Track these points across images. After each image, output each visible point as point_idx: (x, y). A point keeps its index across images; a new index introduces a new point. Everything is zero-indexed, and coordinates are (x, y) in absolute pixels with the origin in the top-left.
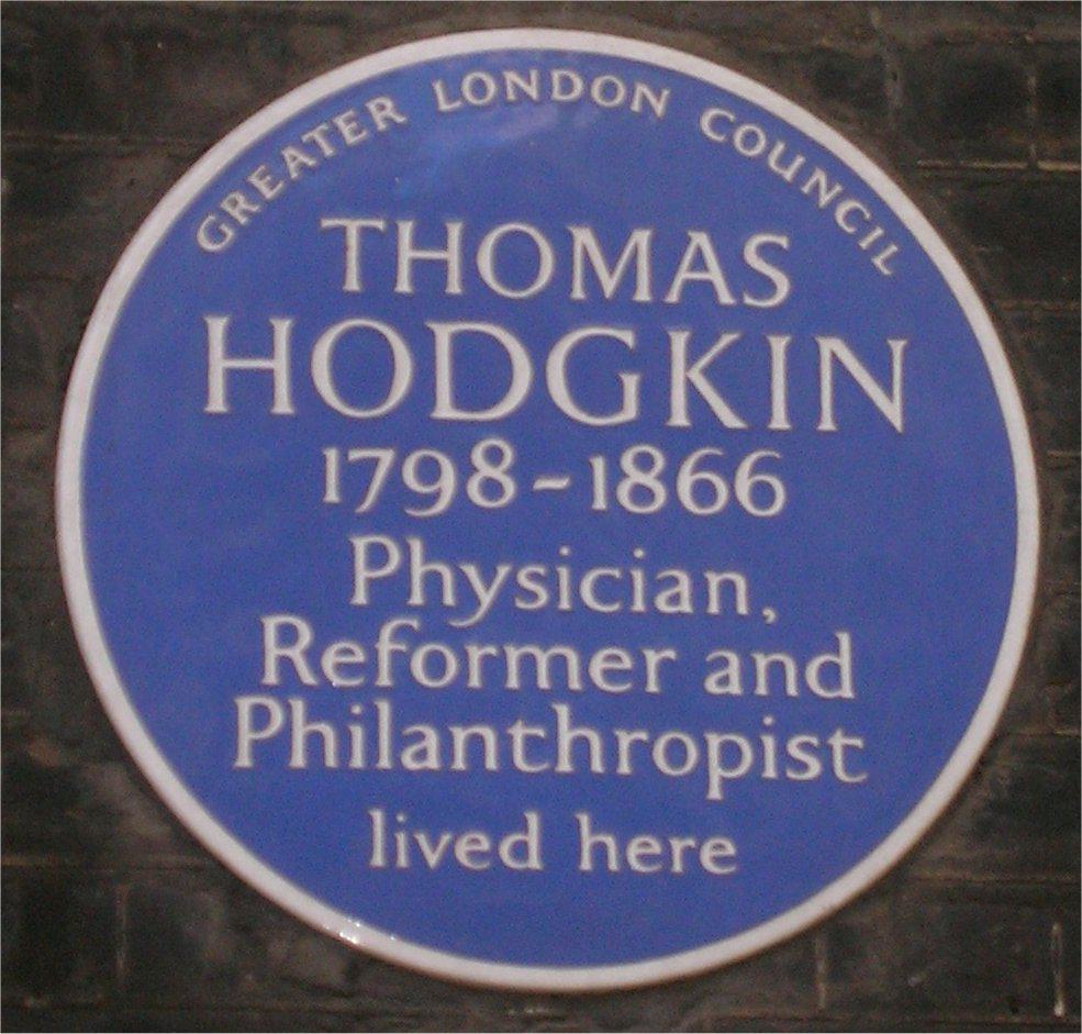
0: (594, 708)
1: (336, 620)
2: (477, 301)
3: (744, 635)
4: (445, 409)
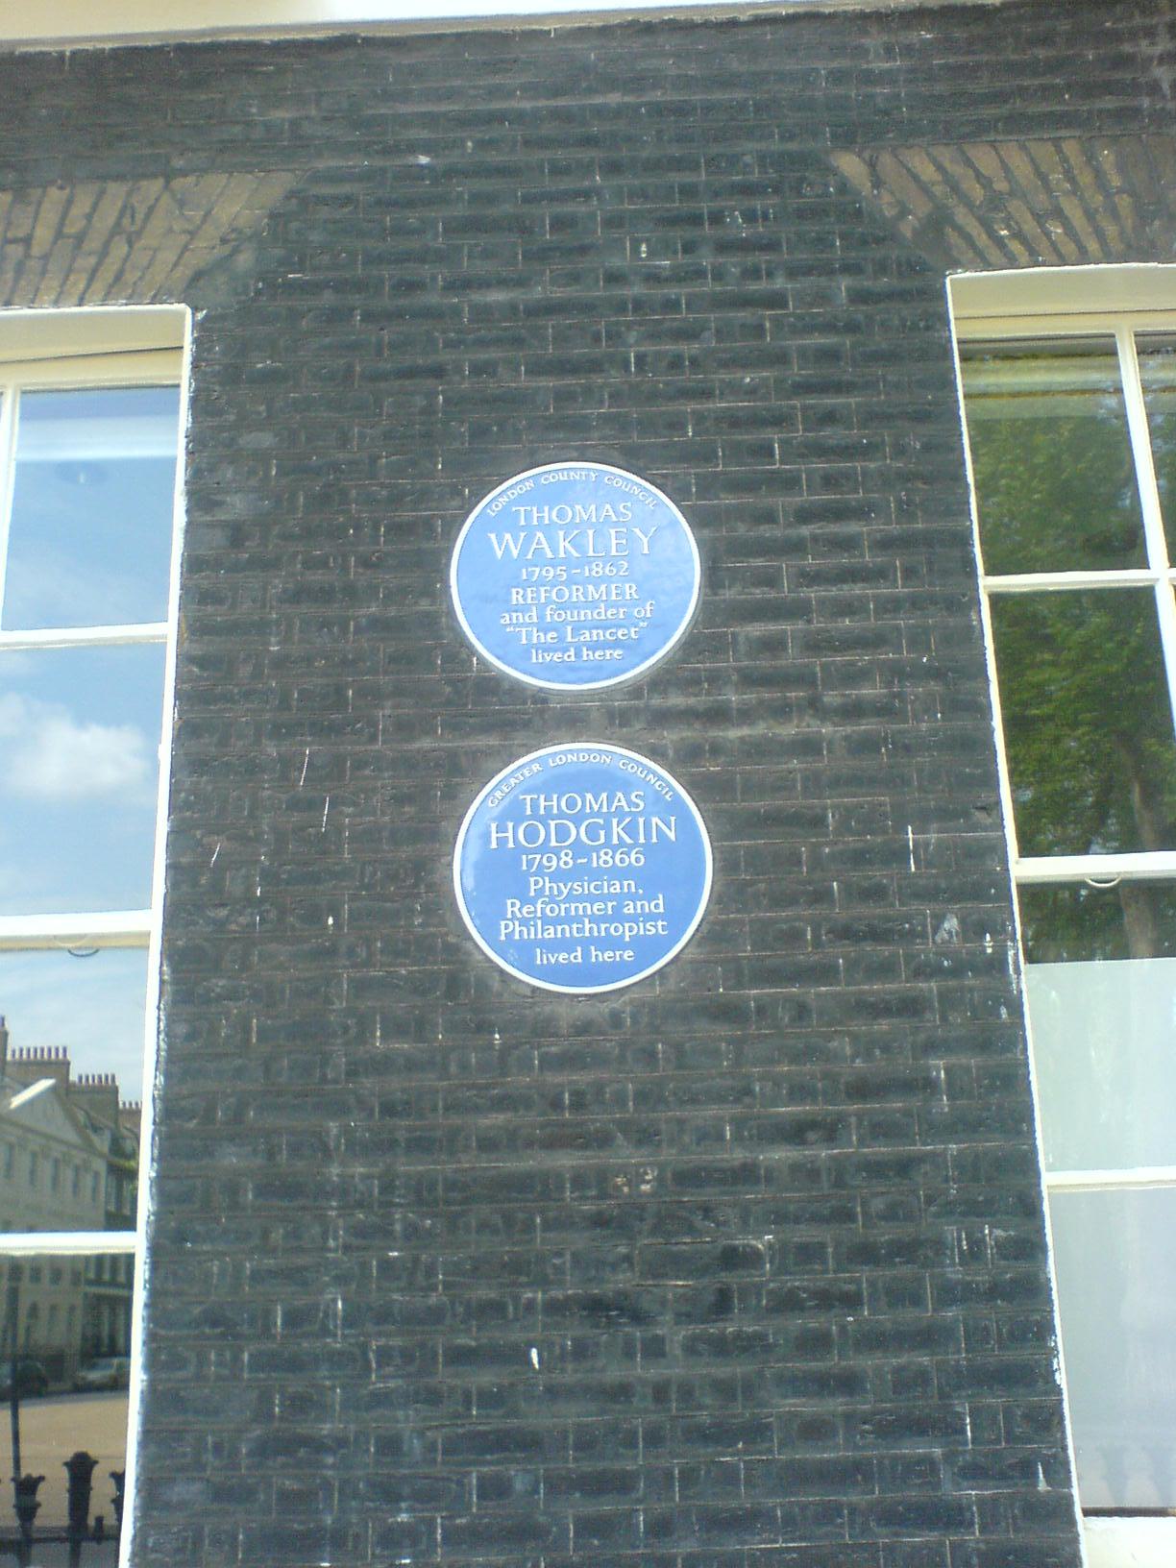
0: (593, 919)
1: (526, 900)
2: (561, 815)
3: (634, 898)
4: (553, 843)
